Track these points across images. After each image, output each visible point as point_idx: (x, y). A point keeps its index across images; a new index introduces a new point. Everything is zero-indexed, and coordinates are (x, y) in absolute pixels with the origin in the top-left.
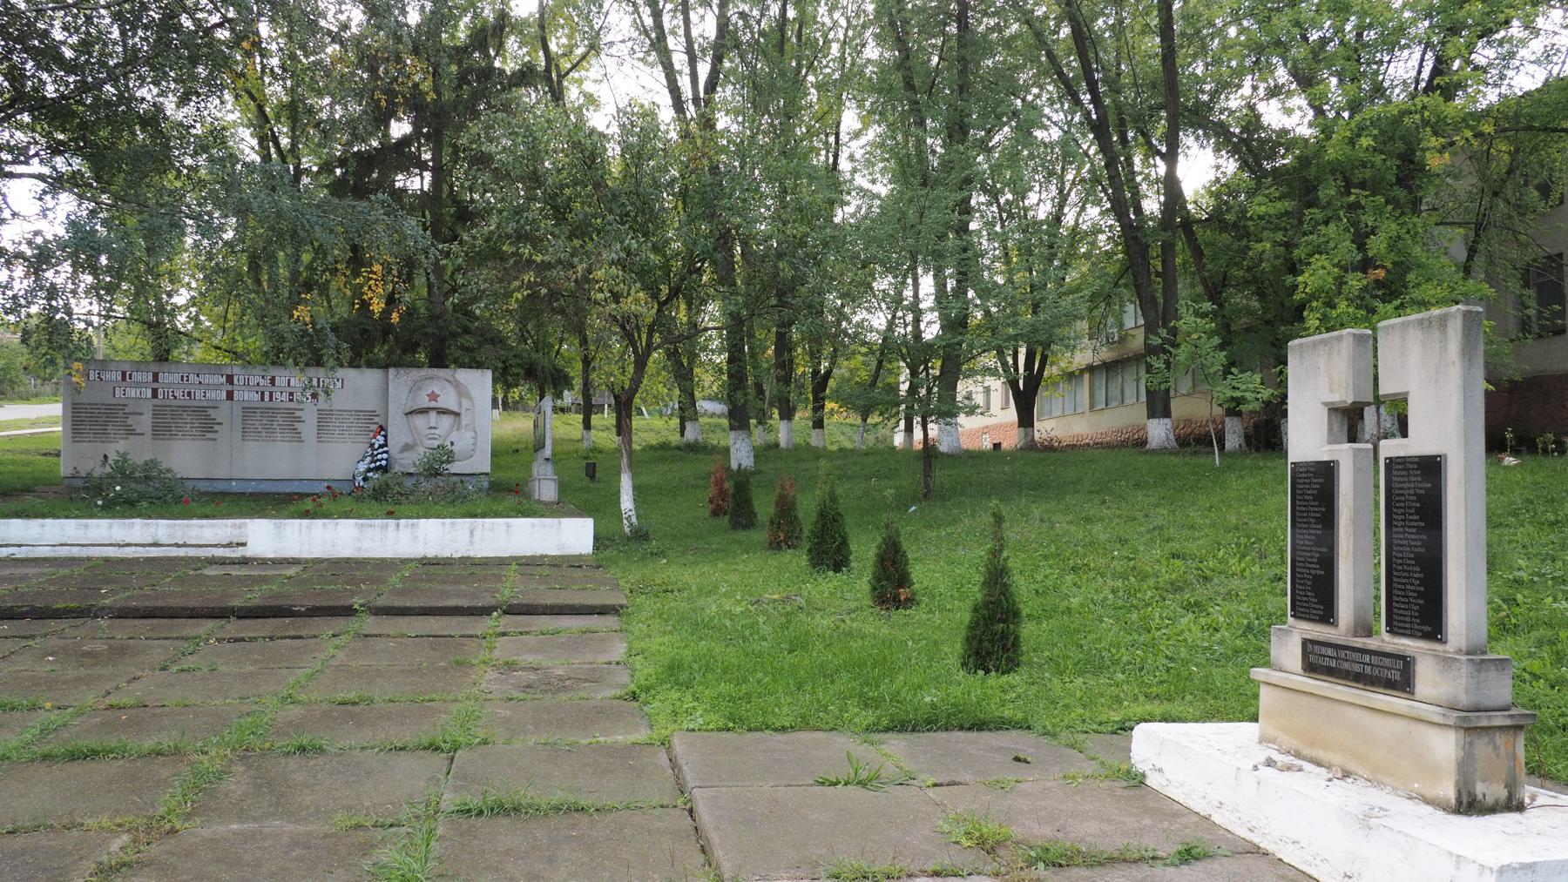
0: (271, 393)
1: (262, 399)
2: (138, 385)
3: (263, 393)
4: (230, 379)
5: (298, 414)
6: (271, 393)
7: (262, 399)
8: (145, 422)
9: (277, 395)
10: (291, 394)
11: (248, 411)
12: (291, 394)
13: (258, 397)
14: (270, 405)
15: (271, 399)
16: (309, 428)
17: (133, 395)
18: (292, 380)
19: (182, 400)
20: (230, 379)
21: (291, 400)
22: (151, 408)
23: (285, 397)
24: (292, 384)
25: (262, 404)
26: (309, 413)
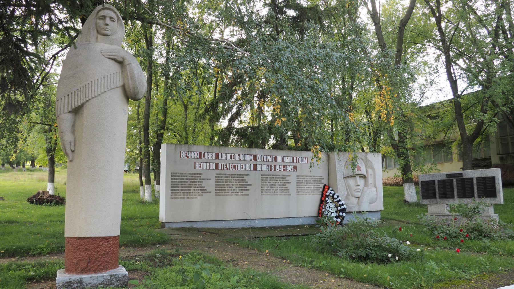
0: (275, 166)
1: (271, 170)
2: (208, 161)
3: (271, 166)
4: (255, 157)
5: (288, 178)
6: (275, 166)
7: (271, 170)
8: (211, 185)
9: (277, 167)
10: (284, 167)
11: (264, 177)
12: (284, 167)
13: (268, 168)
14: (275, 173)
15: (275, 170)
16: (292, 187)
17: (205, 167)
18: (285, 158)
19: (232, 171)
20: (255, 157)
21: (284, 170)
22: (215, 175)
23: (281, 168)
24: (284, 161)
25: (270, 173)
26: (293, 179)
